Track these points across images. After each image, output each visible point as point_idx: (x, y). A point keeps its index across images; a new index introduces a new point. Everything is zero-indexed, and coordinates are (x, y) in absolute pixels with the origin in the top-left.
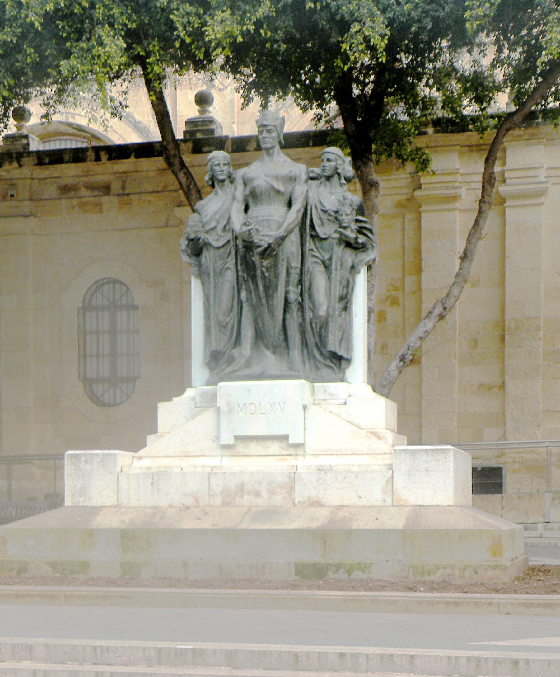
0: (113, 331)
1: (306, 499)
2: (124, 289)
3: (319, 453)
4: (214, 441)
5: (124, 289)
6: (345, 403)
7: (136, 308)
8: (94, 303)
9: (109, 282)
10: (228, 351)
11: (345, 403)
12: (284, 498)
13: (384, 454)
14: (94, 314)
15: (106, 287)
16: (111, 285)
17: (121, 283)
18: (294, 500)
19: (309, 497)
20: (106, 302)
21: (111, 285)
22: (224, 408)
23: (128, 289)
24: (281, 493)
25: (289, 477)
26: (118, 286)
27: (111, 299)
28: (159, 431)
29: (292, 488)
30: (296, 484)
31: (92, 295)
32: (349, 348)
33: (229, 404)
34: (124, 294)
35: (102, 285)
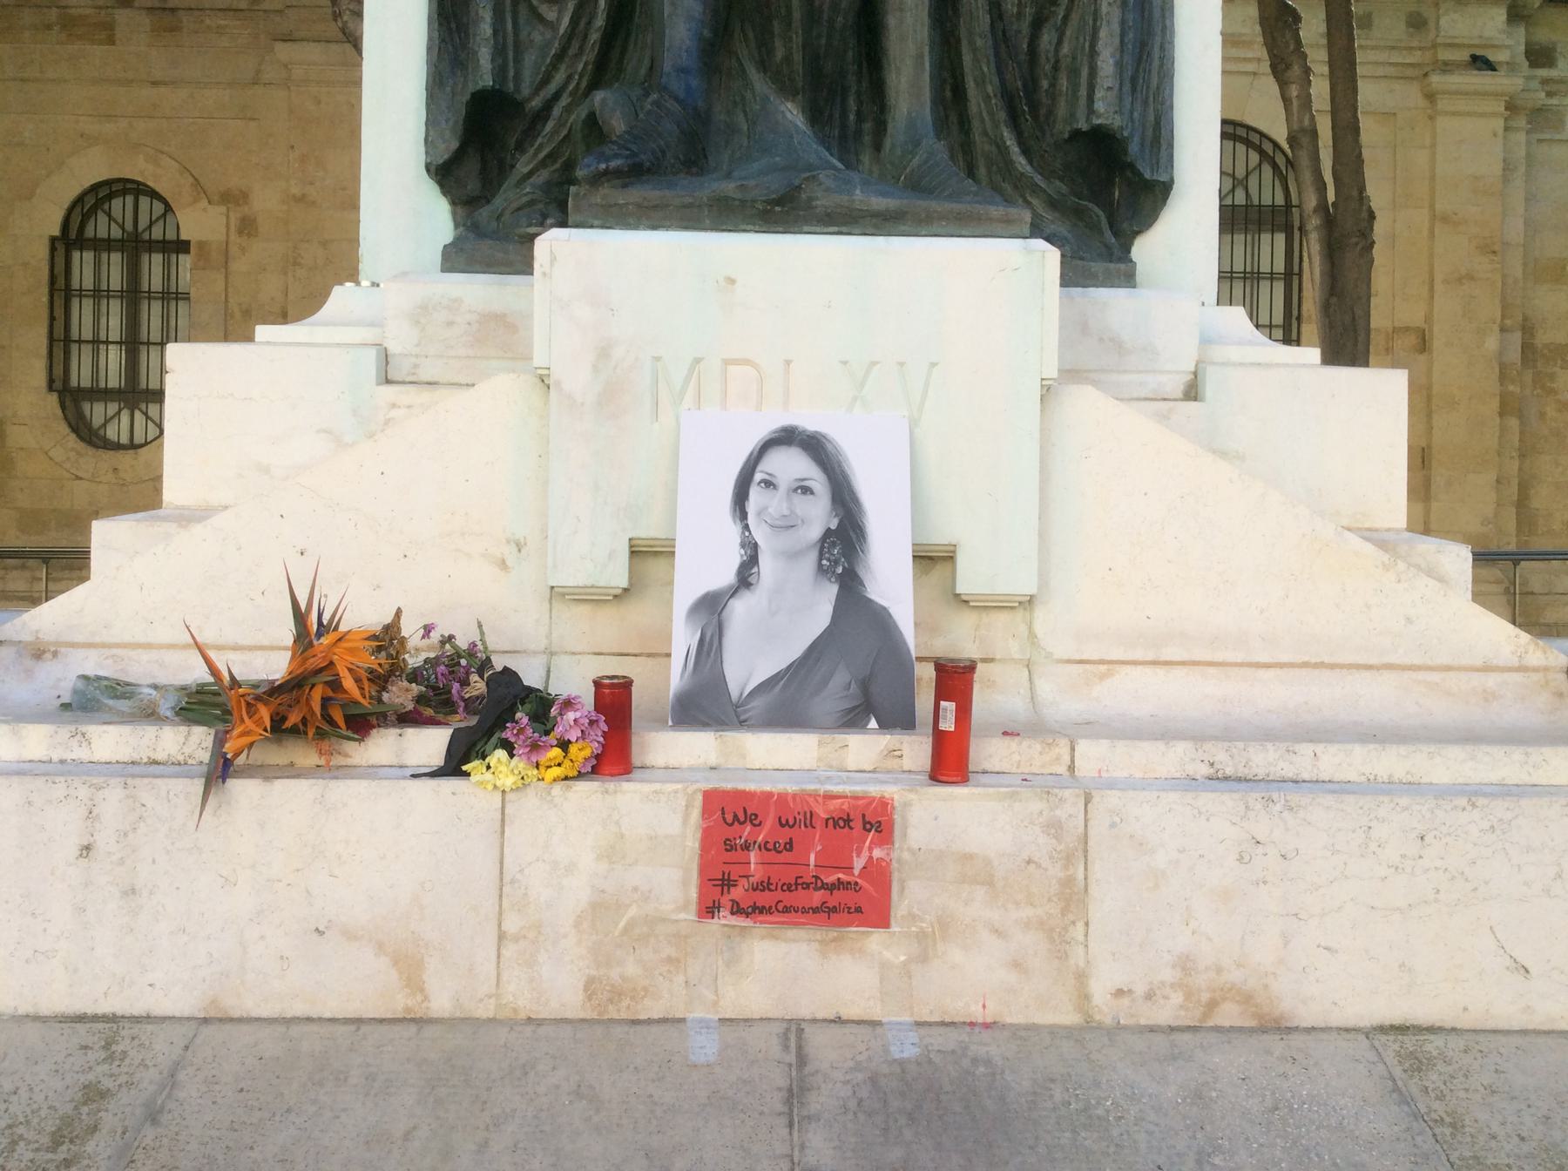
0: (133, 295)
1: (1168, 975)
2: (158, 208)
3: (1117, 654)
4: (503, 565)
5: (158, 208)
6: (1192, 392)
7: (182, 247)
8: (89, 232)
9: (124, 192)
10: (564, 101)
11: (1192, 392)
12: (1016, 965)
13: (1487, 669)
14: (88, 256)
15: (116, 204)
16: (130, 199)
17: (154, 195)
18: (1081, 977)
19: (1185, 964)
20: (116, 233)
21: (130, 199)
22: (575, 377)
23: (168, 208)
24: (998, 932)
25: (1054, 828)
26: (144, 202)
27: (129, 226)
28: (172, 491)
29: (1073, 897)
30: (1097, 869)
31: (85, 218)
32: (1159, 135)
33: (604, 353)
34: (158, 219)
35: (110, 197)
